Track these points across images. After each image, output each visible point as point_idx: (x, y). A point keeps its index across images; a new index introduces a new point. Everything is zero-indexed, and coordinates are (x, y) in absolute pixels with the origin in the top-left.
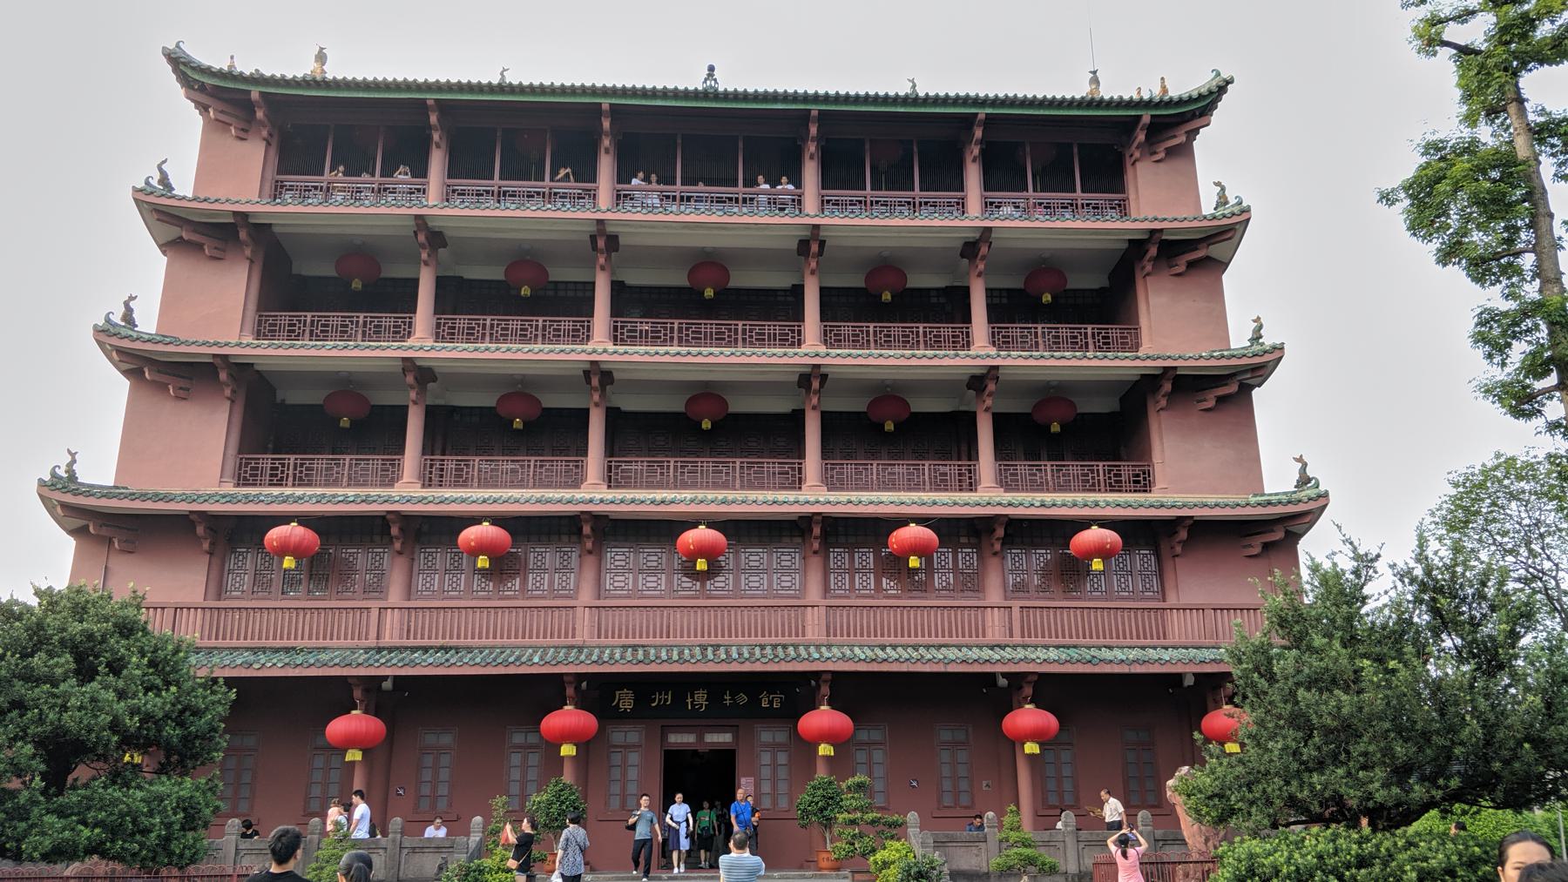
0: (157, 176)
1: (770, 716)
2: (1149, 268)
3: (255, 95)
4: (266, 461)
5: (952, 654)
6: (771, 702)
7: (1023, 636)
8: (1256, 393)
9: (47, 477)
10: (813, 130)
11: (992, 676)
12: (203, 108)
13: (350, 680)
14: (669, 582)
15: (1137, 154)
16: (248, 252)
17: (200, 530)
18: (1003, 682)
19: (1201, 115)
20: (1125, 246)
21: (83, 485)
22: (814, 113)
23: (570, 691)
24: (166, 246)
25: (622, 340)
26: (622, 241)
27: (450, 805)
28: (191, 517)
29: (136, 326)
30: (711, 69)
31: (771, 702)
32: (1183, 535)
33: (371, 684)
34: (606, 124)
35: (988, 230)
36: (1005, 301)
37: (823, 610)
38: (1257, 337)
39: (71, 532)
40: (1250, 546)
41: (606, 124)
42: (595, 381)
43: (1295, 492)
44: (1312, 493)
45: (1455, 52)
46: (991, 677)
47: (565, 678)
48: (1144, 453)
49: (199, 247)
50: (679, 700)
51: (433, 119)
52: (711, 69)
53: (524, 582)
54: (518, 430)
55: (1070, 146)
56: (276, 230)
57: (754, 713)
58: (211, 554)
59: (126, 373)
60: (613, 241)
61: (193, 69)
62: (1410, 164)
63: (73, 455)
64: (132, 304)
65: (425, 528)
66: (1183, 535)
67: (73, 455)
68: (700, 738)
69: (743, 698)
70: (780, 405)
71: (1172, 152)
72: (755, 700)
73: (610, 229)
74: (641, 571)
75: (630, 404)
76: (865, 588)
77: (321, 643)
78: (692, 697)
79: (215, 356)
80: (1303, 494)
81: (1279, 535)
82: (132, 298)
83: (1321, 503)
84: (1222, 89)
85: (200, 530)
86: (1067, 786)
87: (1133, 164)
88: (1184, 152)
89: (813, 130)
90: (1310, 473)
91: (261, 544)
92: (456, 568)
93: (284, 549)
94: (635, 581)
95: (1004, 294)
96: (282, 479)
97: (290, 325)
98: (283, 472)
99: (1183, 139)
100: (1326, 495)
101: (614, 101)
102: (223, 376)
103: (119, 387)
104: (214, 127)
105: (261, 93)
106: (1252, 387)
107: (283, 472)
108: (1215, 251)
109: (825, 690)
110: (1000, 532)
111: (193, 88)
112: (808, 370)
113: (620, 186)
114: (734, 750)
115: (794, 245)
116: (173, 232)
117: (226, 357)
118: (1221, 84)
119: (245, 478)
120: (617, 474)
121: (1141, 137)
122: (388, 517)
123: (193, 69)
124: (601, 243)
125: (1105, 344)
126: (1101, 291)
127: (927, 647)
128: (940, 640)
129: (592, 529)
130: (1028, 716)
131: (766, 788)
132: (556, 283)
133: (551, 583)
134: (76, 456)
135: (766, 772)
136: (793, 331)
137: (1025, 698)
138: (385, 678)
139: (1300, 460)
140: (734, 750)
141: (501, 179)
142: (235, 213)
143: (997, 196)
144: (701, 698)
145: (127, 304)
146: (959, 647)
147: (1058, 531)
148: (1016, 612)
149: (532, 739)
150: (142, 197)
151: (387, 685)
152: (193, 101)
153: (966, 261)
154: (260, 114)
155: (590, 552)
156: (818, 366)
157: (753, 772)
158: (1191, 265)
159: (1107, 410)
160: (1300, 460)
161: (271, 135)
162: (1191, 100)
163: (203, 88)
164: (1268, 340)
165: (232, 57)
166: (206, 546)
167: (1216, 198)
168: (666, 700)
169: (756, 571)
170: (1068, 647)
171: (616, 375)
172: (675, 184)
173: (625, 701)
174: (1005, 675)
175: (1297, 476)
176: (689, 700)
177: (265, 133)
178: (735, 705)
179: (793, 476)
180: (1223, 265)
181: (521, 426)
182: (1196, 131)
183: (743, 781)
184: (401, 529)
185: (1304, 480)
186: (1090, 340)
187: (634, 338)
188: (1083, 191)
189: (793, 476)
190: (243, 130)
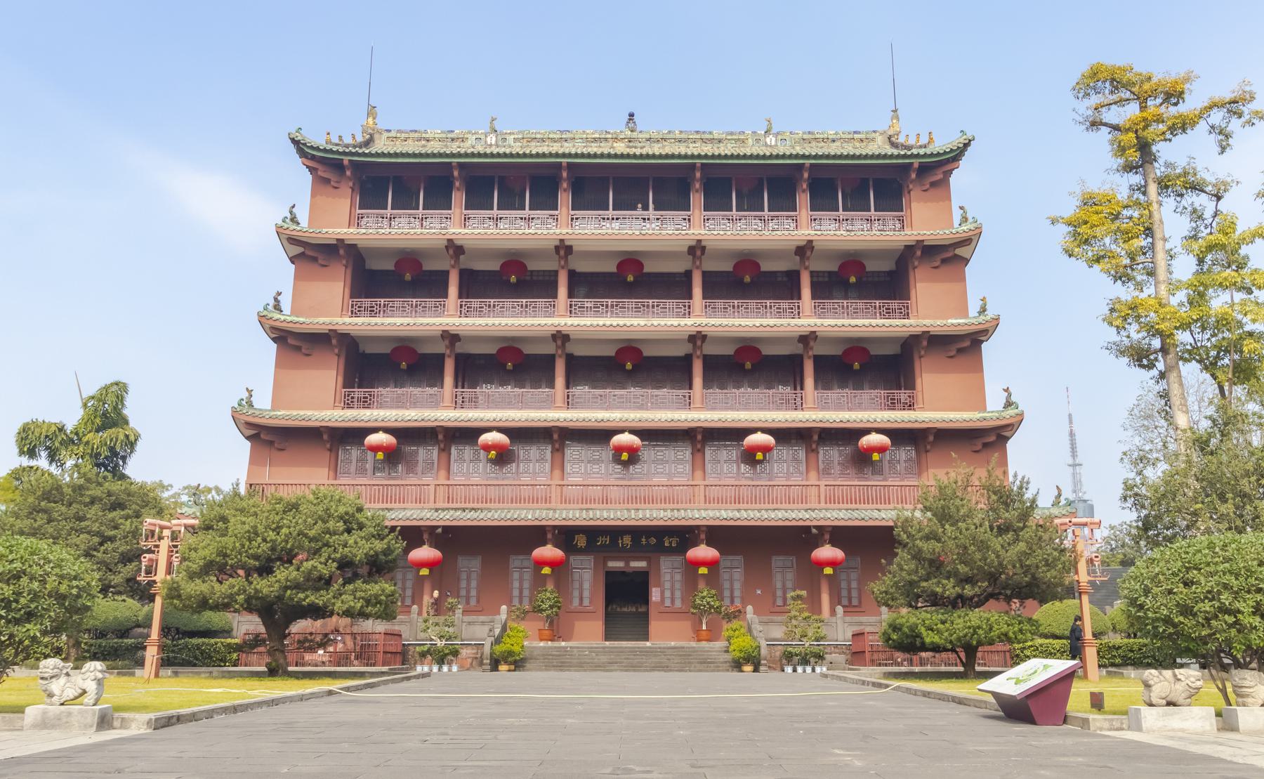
0: (289, 216)
1: (671, 551)
2: (916, 263)
3: (346, 162)
4: (358, 392)
5: (780, 514)
6: (670, 543)
7: (826, 503)
8: (984, 346)
9: (236, 406)
10: (698, 175)
11: (809, 527)
12: (311, 170)
13: (423, 529)
14: (607, 469)
15: (911, 186)
16: (344, 262)
17: (325, 437)
18: (814, 531)
19: (953, 162)
20: (903, 247)
21: (256, 409)
22: (698, 165)
23: (549, 536)
24: (292, 260)
25: (575, 313)
26: (575, 249)
27: (478, 601)
28: (321, 429)
29: (282, 311)
30: (632, 115)
31: (670, 543)
32: (931, 438)
33: (432, 529)
34: (565, 174)
35: (810, 242)
36: (826, 279)
37: (702, 487)
38: (983, 310)
39: (248, 438)
40: (975, 445)
41: (565, 174)
42: (559, 342)
43: (1003, 411)
44: (1011, 412)
45: (1109, 129)
46: (808, 529)
47: (547, 528)
48: (911, 385)
49: (315, 259)
50: (614, 541)
51: (456, 173)
52: (632, 115)
53: (518, 466)
54: (509, 370)
55: (868, 180)
56: (359, 246)
57: (661, 549)
58: (330, 450)
59: (274, 340)
60: (569, 249)
61: (308, 147)
62: (1070, 208)
63: (250, 391)
64: (279, 298)
65: (457, 434)
66: (931, 438)
67: (250, 391)
68: (627, 563)
69: (653, 541)
70: (680, 351)
71: (933, 184)
72: (661, 542)
73: (567, 243)
74: (589, 462)
75: (579, 351)
76: (730, 473)
77: (389, 506)
78: (622, 539)
79: (330, 330)
80: (1008, 412)
81: (992, 438)
82: (279, 294)
83: (1018, 418)
84: (966, 145)
85: (325, 437)
86: (854, 594)
87: (909, 192)
88: (943, 183)
89: (698, 175)
90: (1013, 399)
91: (363, 444)
92: (477, 459)
93: (375, 449)
94: (586, 468)
95: (826, 275)
96: (370, 404)
97: (371, 307)
98: (370, 400)
99: (940, 176)
100: (1021, 415)
101: (570, 160)
102: (334, 341)
103: (270, 348)
104: (320, 183)
105: (349, 160)
106: (982, 342)
107: (370, 400)
108: (960, 251)
109: (703, 536)
110: (816, 437)
111: (306, 157)
112: (695, 333)
113: (573, 212)
114: (647, 573)
115: (686, 249)
116: (298, 250)
117: (336, 330)
118: (967, 141)
119: (348, 404)
120: (573, 400)
121: (913, 176)
122: (438, 429)
123: (308, 147)
124: (562, 253)
125: (889, 314)
126: (890, 273)
127: (767, 510)
128: (775, 506)
129: (559, 436)
130: (827, 552)
131: (668, 594)
132: (532, 271)
133: (534, 469)
134: (253, 393)
135: (667, 585)
136: (685, 306)
137: (825, 541)
138: (437, 527)
139: (1007, 390)
140: (647, 573)
141: (498, 209)
142: (338, 240)
143: (817, 214)
144: (627, 540)
145: (276, 299)
146: (786, 510)
147: (849, 436)
148: (823, 488)
149: (526, 563)
150: (280, 230)
151: (440, 530)
152: (308, 167)
153: (798, 258)
154: (348, 173)
155: (558, 450)
156: (701, 332)
157: (658, 585)
158: (944, 261)
159: (892, 353)
160: (1007, 390)
161: (354, 184)
162: (945, 153)
163: (313, 158)
164: (990, 314)
165: (328, 134)
166: (328, 446)
167: (960, 217)
168: (606, 541)
169: (663, 462)
170: (853, 510)
171: (571, 337)
172: (608, 210)
173: (581, 541)
174: (816, 527)
175: (1004, 401)
176: (620, 541)
177: (351, 184)
178: (648, 544)
179: (685, 401)
180: (966, 261)
181: (511, 368)
182: (951, 172)
183: (654, 589)
184: (444, 436)
185: (1009, 404)
186: (878, 311)
187: (582, 311)
188: (875, 211)
189: (685, 401)
190: (337, 182)
